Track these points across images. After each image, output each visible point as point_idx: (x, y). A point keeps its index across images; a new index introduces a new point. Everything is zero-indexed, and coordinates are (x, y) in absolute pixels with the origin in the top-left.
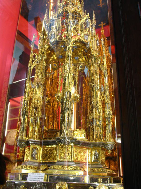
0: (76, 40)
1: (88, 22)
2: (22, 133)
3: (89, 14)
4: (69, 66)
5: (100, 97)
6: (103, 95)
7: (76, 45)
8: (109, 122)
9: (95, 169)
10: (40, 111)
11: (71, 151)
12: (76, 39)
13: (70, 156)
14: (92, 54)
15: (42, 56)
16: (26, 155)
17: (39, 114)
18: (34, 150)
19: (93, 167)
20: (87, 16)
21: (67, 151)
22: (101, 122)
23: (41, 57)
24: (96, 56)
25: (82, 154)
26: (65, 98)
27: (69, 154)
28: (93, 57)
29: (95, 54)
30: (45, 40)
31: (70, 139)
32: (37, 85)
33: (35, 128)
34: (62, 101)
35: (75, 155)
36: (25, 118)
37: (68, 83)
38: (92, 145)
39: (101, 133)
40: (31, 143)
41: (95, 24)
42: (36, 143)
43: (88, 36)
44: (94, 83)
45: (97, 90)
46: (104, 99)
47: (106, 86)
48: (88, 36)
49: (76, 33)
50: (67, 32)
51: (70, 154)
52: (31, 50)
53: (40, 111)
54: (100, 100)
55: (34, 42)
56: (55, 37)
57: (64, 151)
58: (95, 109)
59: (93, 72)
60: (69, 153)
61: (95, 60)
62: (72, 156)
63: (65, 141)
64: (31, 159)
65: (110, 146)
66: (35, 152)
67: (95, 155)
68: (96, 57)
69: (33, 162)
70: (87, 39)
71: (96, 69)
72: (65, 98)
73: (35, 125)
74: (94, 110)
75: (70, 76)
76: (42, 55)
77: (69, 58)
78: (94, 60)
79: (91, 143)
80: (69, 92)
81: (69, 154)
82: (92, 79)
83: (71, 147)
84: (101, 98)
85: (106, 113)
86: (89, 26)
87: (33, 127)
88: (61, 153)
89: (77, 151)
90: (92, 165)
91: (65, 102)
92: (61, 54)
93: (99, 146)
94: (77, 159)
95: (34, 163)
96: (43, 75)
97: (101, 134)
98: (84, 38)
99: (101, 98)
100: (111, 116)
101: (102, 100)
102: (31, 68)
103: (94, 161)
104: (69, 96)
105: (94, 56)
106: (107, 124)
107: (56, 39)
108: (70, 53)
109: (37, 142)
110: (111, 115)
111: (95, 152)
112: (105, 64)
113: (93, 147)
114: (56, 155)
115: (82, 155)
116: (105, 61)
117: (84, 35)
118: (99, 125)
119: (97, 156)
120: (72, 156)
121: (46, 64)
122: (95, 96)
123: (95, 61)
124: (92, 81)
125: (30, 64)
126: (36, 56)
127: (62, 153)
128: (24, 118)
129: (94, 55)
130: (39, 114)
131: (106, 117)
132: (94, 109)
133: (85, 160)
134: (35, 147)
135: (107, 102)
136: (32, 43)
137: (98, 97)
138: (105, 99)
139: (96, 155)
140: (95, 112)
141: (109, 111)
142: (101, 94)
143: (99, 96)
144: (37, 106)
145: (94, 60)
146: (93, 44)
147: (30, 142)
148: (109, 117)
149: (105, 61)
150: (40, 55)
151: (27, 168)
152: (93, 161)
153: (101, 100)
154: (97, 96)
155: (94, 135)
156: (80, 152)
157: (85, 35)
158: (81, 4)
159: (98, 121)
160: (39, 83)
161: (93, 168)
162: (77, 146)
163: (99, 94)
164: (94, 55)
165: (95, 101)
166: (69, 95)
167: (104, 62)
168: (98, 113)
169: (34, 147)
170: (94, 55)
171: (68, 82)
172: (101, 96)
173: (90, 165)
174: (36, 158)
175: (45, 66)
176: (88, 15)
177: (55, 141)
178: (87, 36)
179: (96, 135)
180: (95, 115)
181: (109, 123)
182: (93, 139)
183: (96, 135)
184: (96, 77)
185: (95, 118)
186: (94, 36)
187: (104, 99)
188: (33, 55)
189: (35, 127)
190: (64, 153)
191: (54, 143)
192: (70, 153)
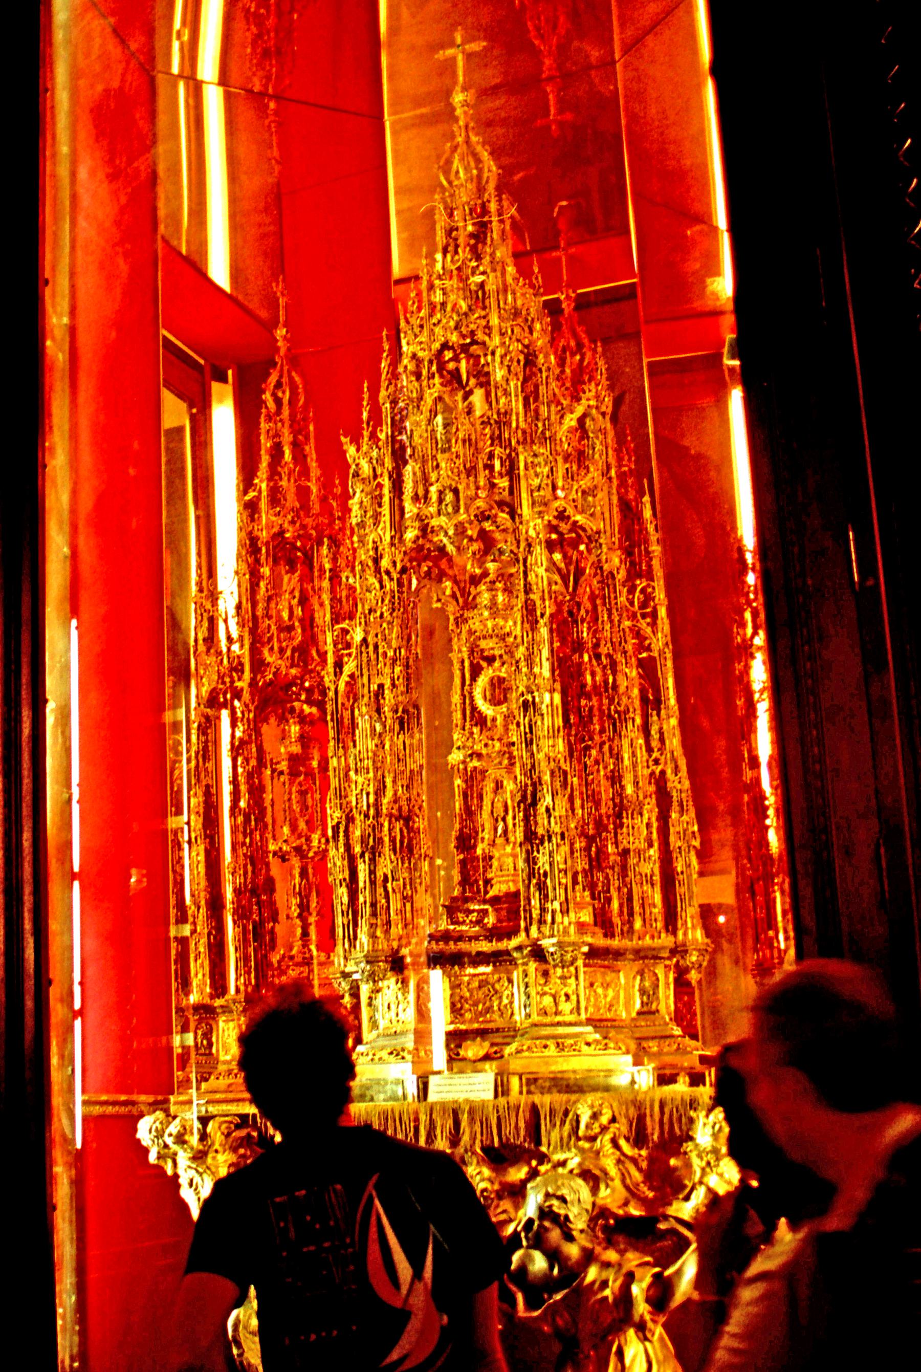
6: (655, 755)
11: (574, 987)
19: (638, 1035)
25: (600, 991)
44: (618, 703)
46: (663, 772)
51: (574, 998)
54: (646, 772)
60: (570, 992)
62: (578, 1002)
67: (643, 991)
84: (651, 763)
87: (405, 898)
93: (656, 958)
99: (651, 763)
101: (652, 774)
103: (639, 1013)
105: (614, 578)
111: (641, 980)
114: (511, 1003)
120: (578, 1002)
138: (669, 771)
142: (650, 750)
144: (410, 811)
152: (634, 1015)
172: (650, 756)
180: (632, 839)
182: (631, 929)
187: (663, 772)
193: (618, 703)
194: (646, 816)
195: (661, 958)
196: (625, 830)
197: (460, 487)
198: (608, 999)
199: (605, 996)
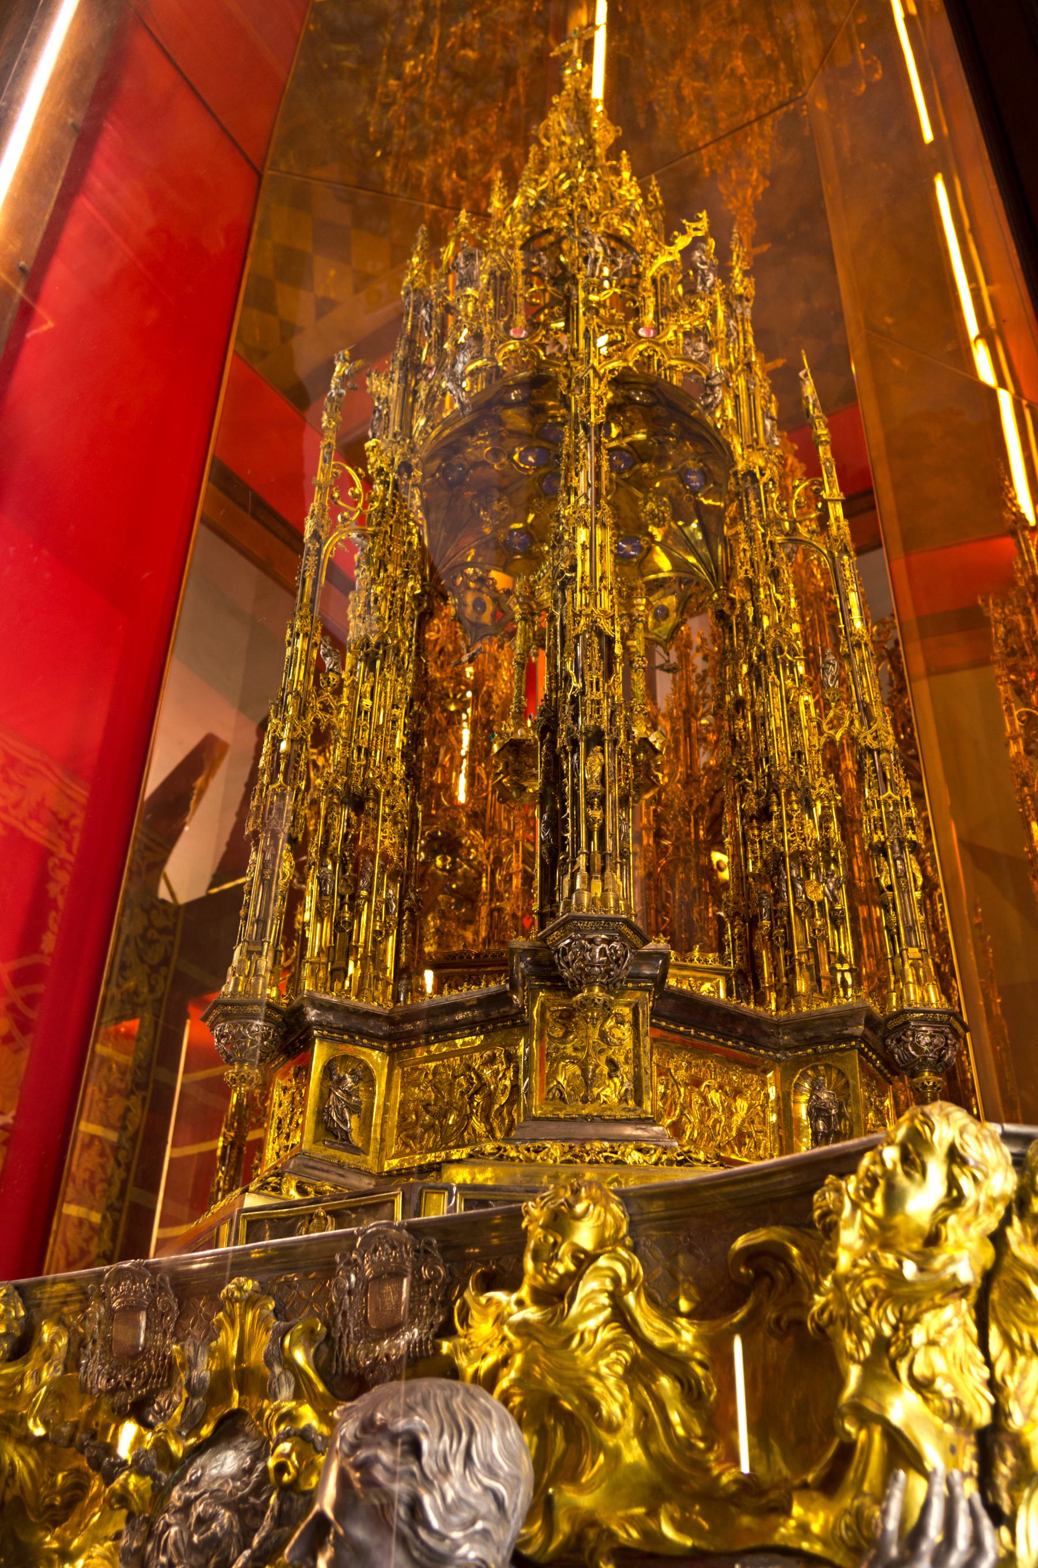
0: (631, 364)
1: (703, 263)
2: (250, 953)
3: (709, 217)
4: (589, 485)
5: (819, 725)
7: (628, 439)
8: (901, 876)
10: (384, 820)
11: (628, 1043)
12: (625, 360)
13: (628, 1085)
14: (741, 466)
15: (396, 486)
16: (279, 1128)
17: (380, 834)
18: (341, 1080)
20: (696, 229)
22: (838, 887)
23: (388, 496)
24: (765, 479)
25: (715, 1097)
26: (572, 672)
27: (612, 1064)
28: (748, 485)
29: (761, 470)
30: (415, 392)
31: (621, 934)
32: (367, 655)
33: (351, 934)
34: (548, 720)
35: (664, 1095)
36: (274, 856)
37: (587, 582)
39: (842, 960)
40: (320, 1025)
41: (748, 300)
42: (354, 1021)
43: (710, 345)
45: (789, 682)
47: (858, 645)
48: (710, 345)
49: (627, 325)
50: (567, 321)
51: (626, 1069)
52: (323, 444)
53: (384, 820)
54: (818, 742)
55: (340, 395)
56: (487, 350)
57: (576, 1049)
58: (788, 795)
59: (750, 575)
61: (759, 505)
62: (637, 1080)
63: (582, 948)
64: (315, 1142)
65: (927, 1039)
66: (348, 1094)
68: (766, 484)
69: (333, 1165)
70: (701, 360)
71: (774, 556)
72: (572, 672)
73: (351, 909)
74: (779, 804)
75: (599, 542)
76: (395, 482)
77: (589, 440)
78: (753, 503)
79: (777, 1025)
80: (600, 633)
82: (751, 615)
83: (629, 1017)
85: (876, 814)
86: (709, 283)
89: (677, 1068)
91: (574, 700)
92: (524, 521)
95: (341, 1172)
96: (402, 600)
97: (846, 967)
98: (686, 353)
99: (825, 727)
100: (910, 835)
102: (322, 545)
104: (601, 658)
105: (755, 481)
106: (890, 888)
107: (493, 359)
108: (593, 407)
109: (369, 1015)
110: (913, 829)
112: (837, 519)
113: (797, 1048)
115: (715, 1108)
116: (834, 501)
117: (680, 335)
118: (821, 904)
119: (828, 1121)
121: (424, 579)
122: (778, 714)
123: (761, 512)
124: (751, 629)
125: (317, 524)
126: (354, 486)
128: (268, 857)
129: (753, 475)
130: (380, 838)
131: (876, 839)
132: (779, 797)
133: (740, 1151)
134: (345, 1058)
135: (875, 745)
136: (331, 400)
137: (804, 723)
140: (790, 818)
141: (896, 804)
143: (810, 719)
145: (753, 503)
146: (744, 410)
147: (312, 1014)
148: (901, 842)
149: (834, 501)
150: (385, 483)
151: (285, 1187)
153: (823, 740)
154: (793, 714)
155: (791, 972)
156: (697, 1083)
157: (686, 334)
158: (644, 195)
159: (813, 877)
160: (377, 646)
162: (672, 1031)
163: (807, 707)
164: (757, 471)
165: (781, 750)
166: (600, 651)
167: (830, 505)
168: (809, 824)
169: (340, 1054)
170: (757, 471)
171: (588, 573)
174: (356, 1138)
175: (418, 591)
176: (699, 219)
177: (506, 992)
178: (702, 346)
179: (809, 968)
180: (787, 837)
181: (898, 878)
183: (807, 974)
184: (778, 602)
185: (794, 856)
186: (749, 365)
188: (339, 472)
189: (351, 924)
191: (494, 1014)
192: (622, 1059)
193: (763, 642)
194: (817, 810)
195: (849, 1038)
196: (774, 823)
197: (486, 329)
198: (736, 1120)
199: (730, 1113)
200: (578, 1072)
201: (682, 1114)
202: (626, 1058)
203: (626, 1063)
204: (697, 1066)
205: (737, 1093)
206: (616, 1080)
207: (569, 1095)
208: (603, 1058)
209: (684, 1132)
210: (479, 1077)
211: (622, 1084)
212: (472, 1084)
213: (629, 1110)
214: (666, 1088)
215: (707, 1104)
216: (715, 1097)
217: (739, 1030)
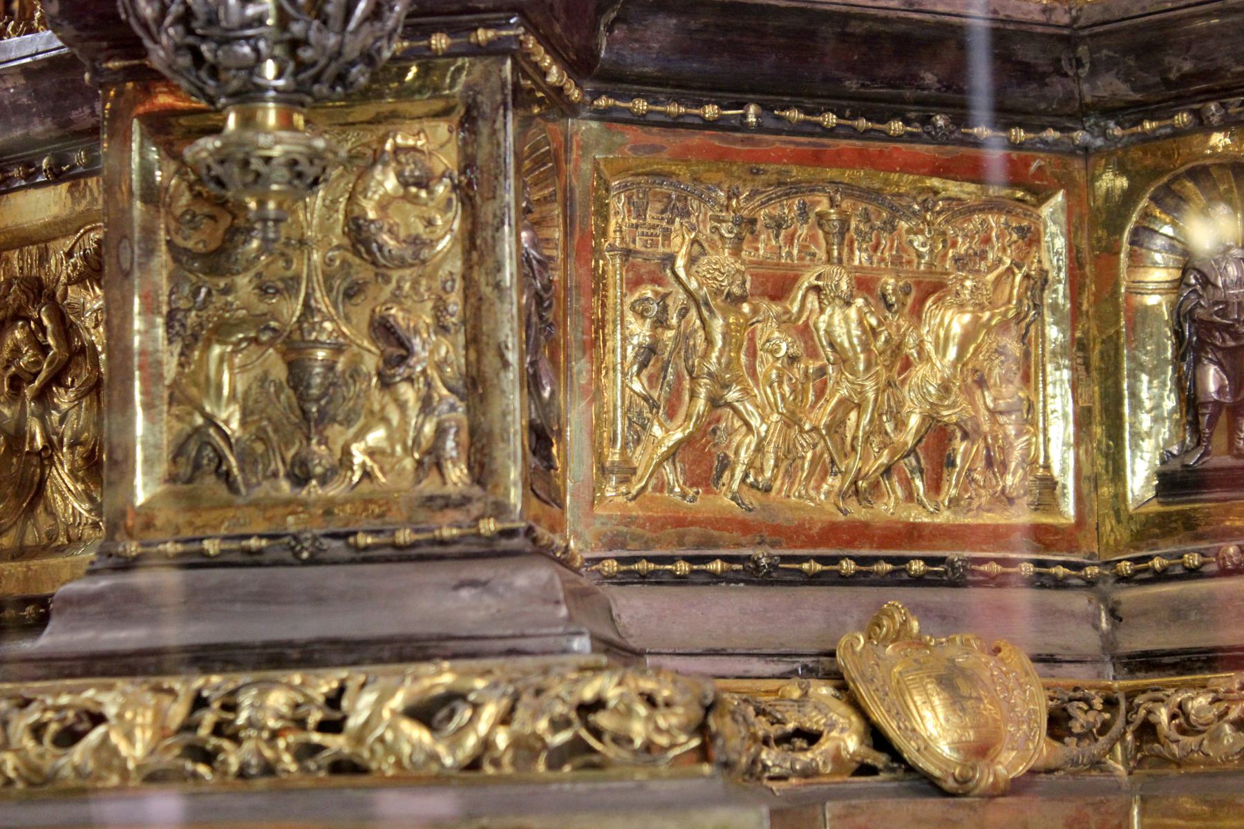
9: (1199, 702)
21: (362, 271)
25: (842, 323)
35: (650, 352)
38: (1112, 86)
57: (264, 290)
60: (414, 318)
81: (394, 342)
88: (192, 342)
90: (1129, 595)
94: (702, 459)
113: (1139, 110)
115: (843, 360)
127: (222, 331)
133: (935, 486)
139: (1204, 328)
152: (1139, 478)
161: (1147, 662)
162: (674, 124)
173: (1079, 601)
190: (261, 330)
200: (279, 372)
201: (715, 402)
202: (440, 309)
203: (442, 329)
204: (778, 224)
205: (931, 288)
206: (408, 393)
207: (247, 459)
208: (362, 313)
209: (726, 464)
210: (66, 329)
211: (427, 405)
212: (44, 349)
213: (447, 503)
214: (660, 322)
215: (813, 354)
216: (842, 323)
217: (929, 78)
